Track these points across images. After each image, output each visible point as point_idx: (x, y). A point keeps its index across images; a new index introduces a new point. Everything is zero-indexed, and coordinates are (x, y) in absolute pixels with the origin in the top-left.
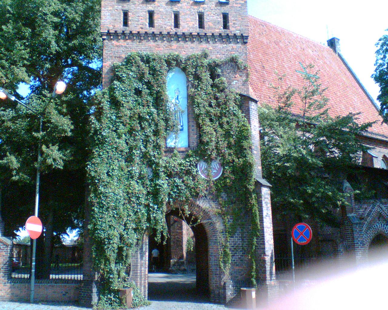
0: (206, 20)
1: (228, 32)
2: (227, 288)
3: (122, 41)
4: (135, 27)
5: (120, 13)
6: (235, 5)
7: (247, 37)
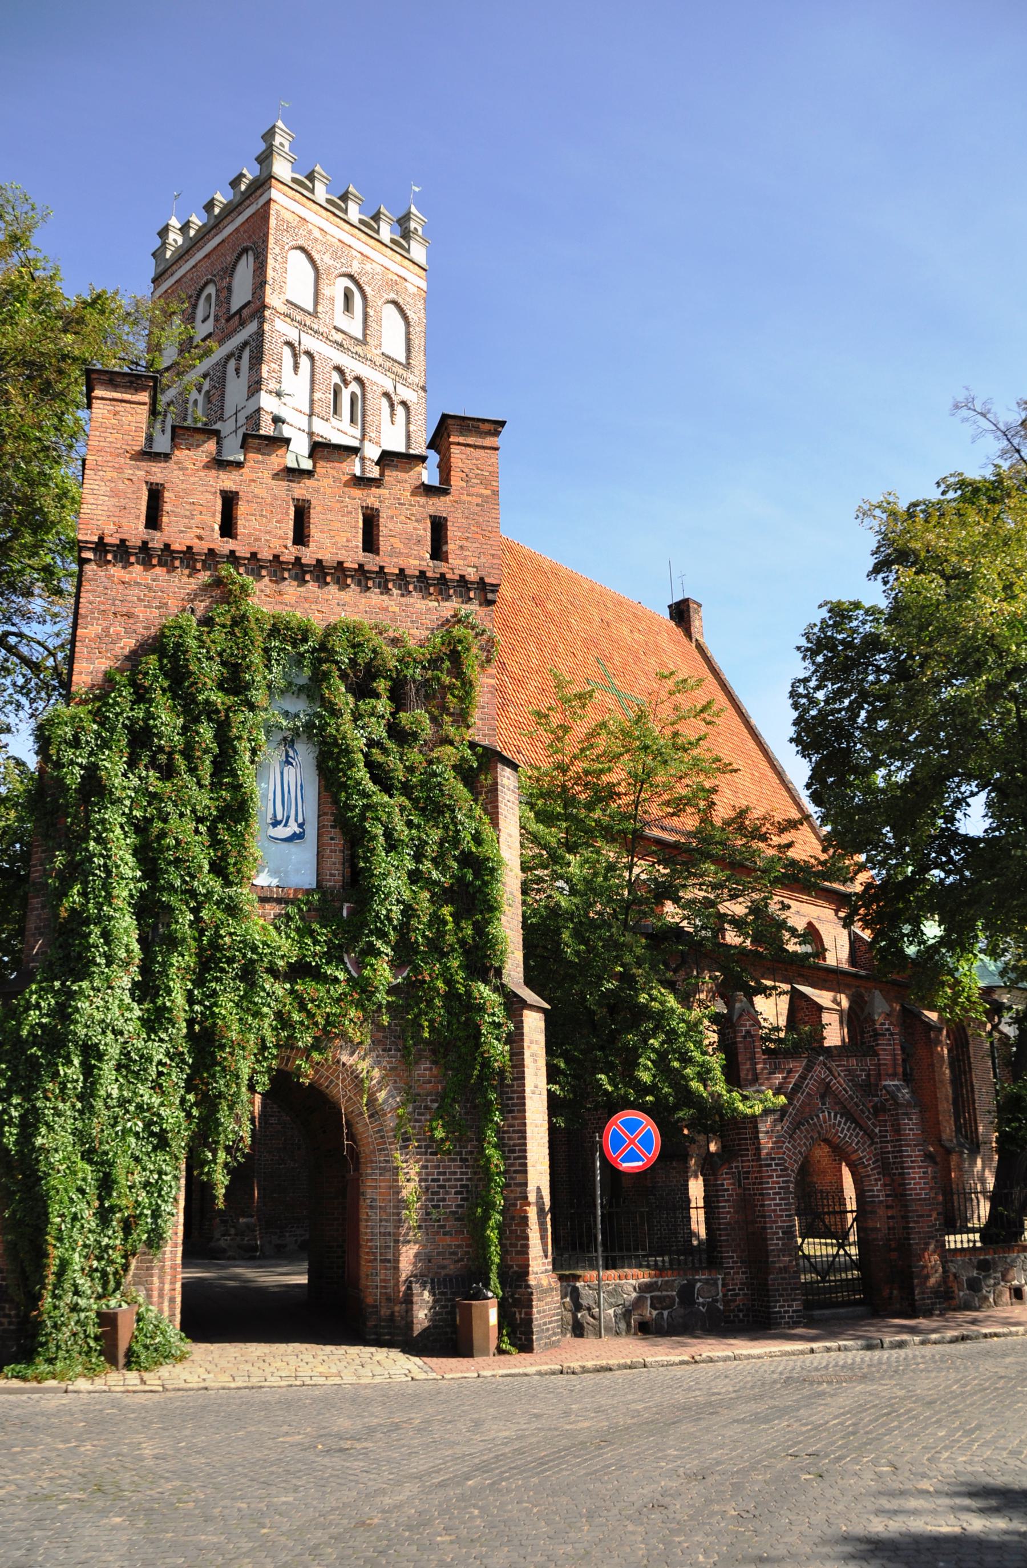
0: (383, 531)
1: (444, 570)
2: (415, 1299)
3: (138, 568)
4: (182, 532)
5: (139, 489)
6: (465, 498)
7: (495, 588)
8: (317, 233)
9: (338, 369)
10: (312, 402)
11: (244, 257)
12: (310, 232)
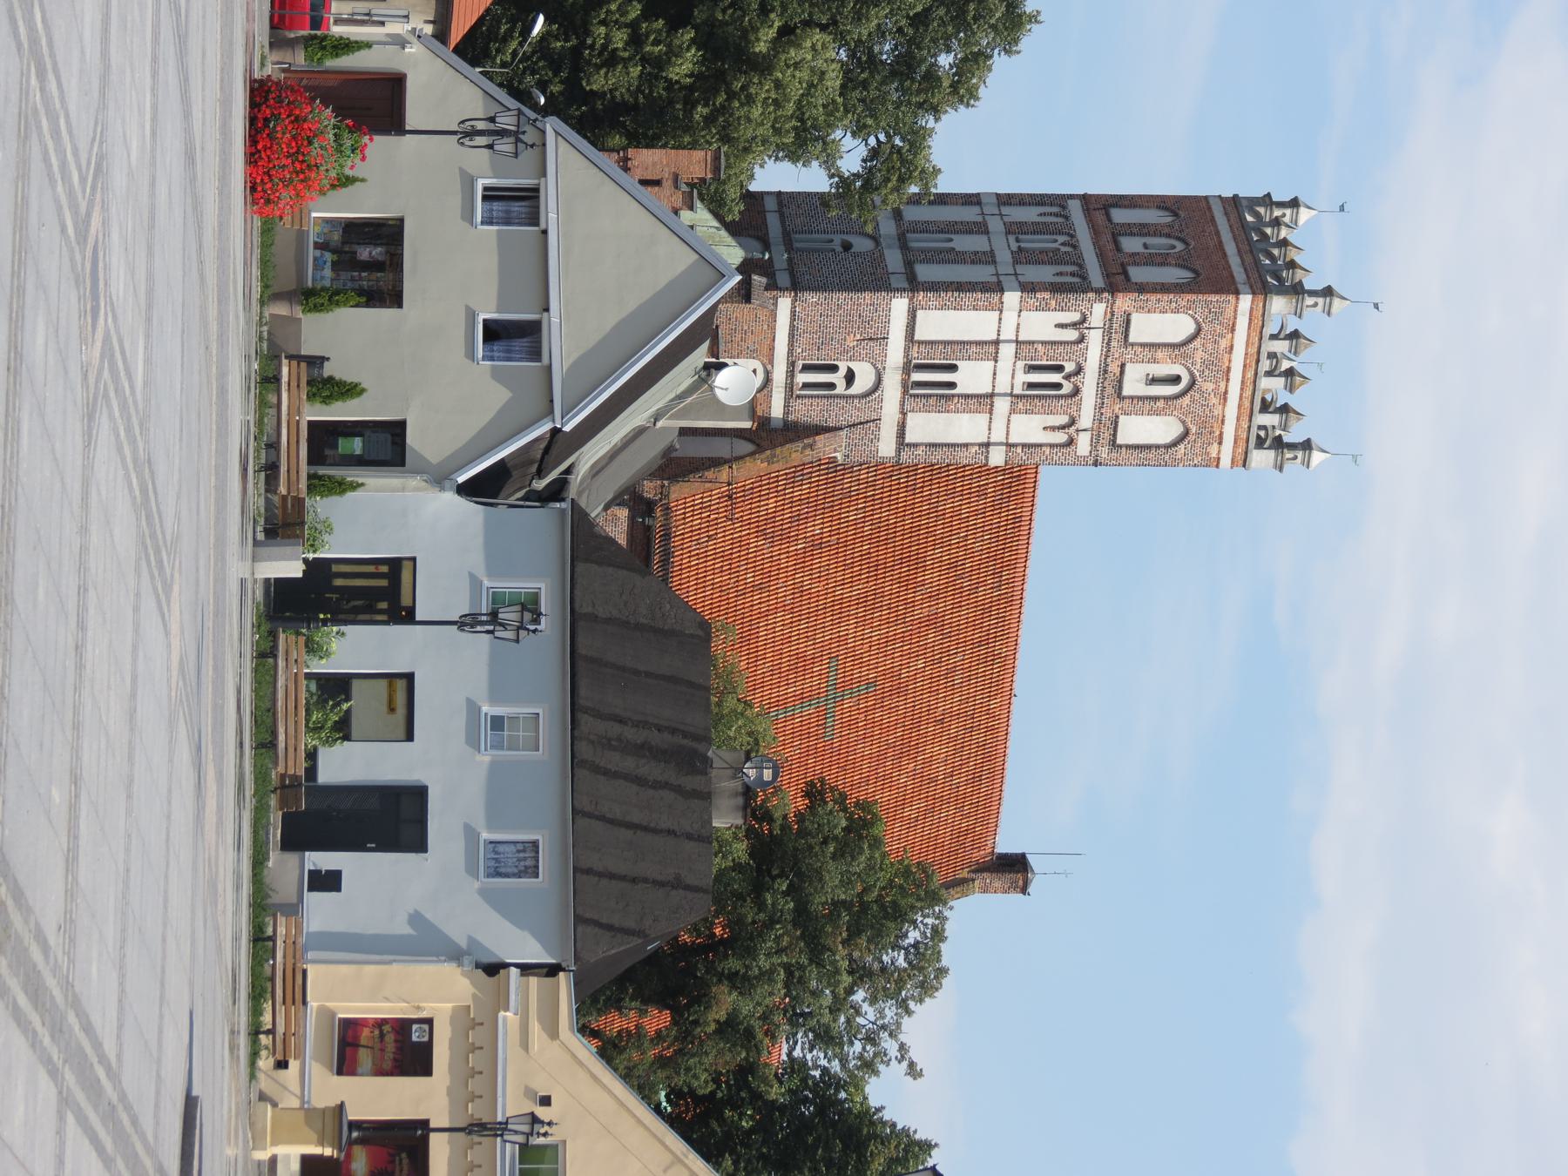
8: (1224, 343)
9: (1079, 370)
10: (1032, 343)
11: (1193, 276)
12: (1222, 336)
